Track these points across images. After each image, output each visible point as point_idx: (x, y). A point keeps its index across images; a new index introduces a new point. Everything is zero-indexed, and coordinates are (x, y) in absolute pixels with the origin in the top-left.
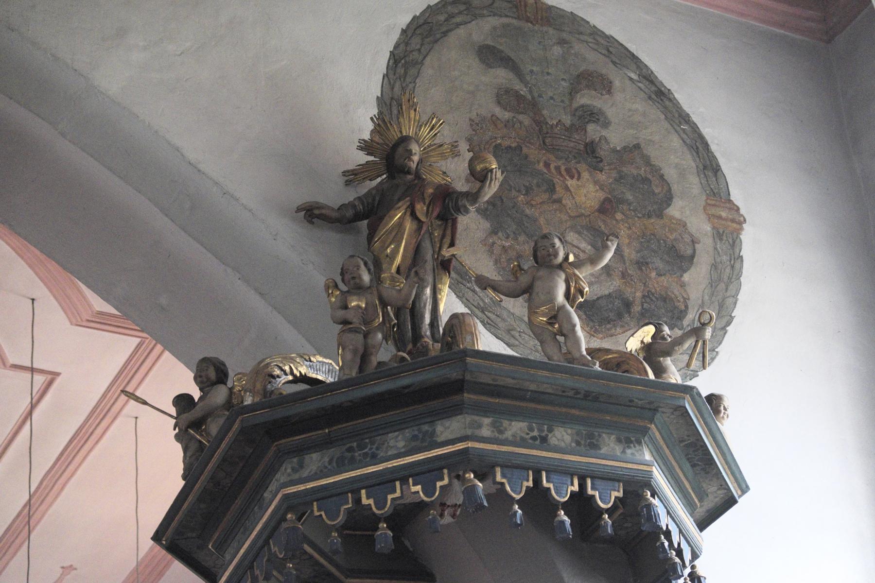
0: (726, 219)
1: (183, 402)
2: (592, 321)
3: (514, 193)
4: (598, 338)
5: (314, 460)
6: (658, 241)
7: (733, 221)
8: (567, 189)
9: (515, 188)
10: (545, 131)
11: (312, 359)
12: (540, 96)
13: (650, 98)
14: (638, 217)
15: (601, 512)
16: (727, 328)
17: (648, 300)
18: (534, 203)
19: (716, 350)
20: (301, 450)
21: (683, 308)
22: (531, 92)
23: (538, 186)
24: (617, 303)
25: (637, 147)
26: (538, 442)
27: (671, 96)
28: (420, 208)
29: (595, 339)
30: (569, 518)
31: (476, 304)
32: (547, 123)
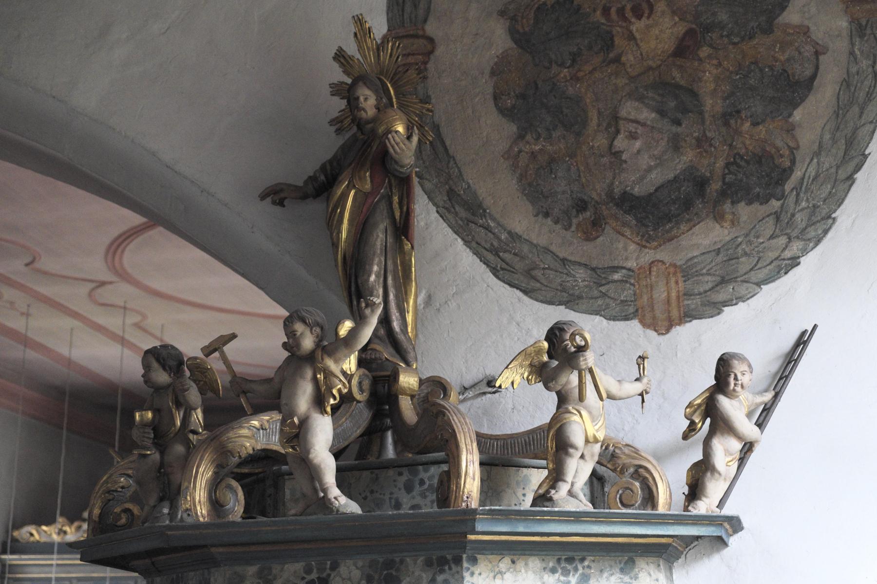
3: (555, 69)
4: (650, 248)
6: (761, 70)
8: (631, 37)
9: (556, 63)
14: (735, 44)
16: (855, 176)
17: (733, 168)
18: (581, 74)
19: (833, 215)
21: (788, 164)
23: (590, 48)
24: (686, 188)
29: (647, 250)
31: (488, 246)
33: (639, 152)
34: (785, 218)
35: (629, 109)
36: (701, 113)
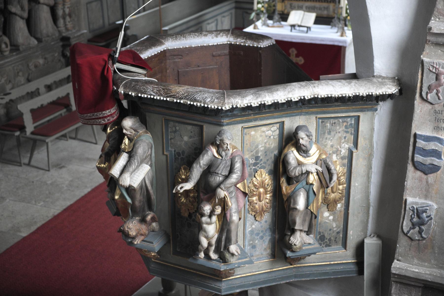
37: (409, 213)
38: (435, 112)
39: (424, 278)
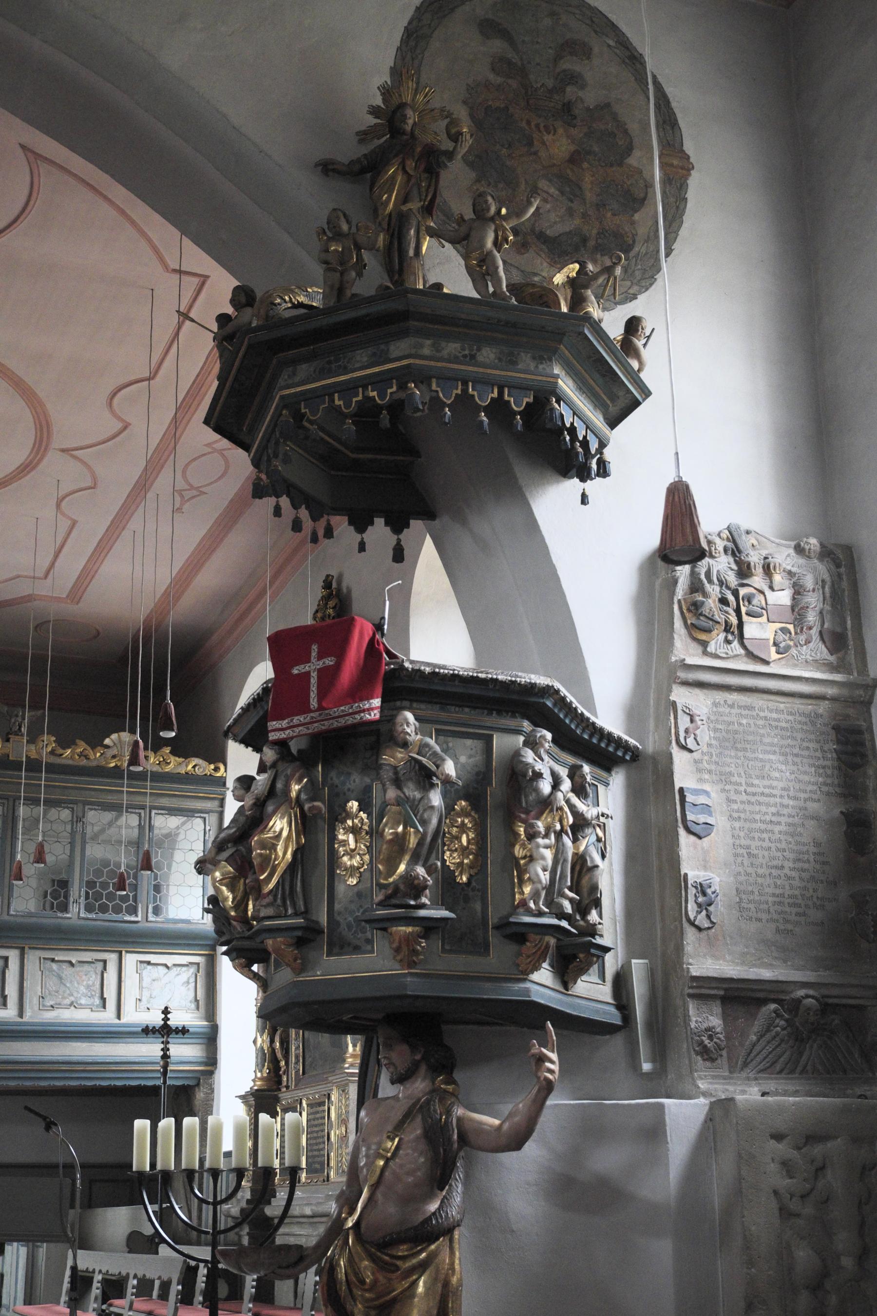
0: (676, 167)
1: (223, 319)
2: (554, 254)
3: (498, 147)
5: (304, 369)
7: (682, 168)
8: (543, 143)
10: (530, 93)
11: (309, 290)
12: (529, 63)
13: (624, 62)
15: (515, 413)
20: (295, 362)
21: (631, 242)
22: (521, 59)
25: (608, 105)
26: (468, 359)
27: (642, 61)
28: (410, 164)
30: (488, 418)
32: (532, 87)
33: (549, 211)
34: (630, 271)
35: (543, 184)
36: (584, 199)
37: (692, 891)
38: (696, 762)
39: (728, 976)
